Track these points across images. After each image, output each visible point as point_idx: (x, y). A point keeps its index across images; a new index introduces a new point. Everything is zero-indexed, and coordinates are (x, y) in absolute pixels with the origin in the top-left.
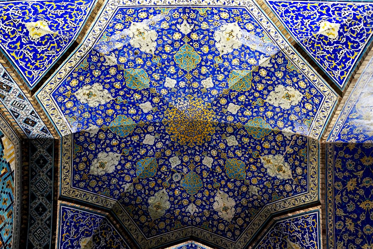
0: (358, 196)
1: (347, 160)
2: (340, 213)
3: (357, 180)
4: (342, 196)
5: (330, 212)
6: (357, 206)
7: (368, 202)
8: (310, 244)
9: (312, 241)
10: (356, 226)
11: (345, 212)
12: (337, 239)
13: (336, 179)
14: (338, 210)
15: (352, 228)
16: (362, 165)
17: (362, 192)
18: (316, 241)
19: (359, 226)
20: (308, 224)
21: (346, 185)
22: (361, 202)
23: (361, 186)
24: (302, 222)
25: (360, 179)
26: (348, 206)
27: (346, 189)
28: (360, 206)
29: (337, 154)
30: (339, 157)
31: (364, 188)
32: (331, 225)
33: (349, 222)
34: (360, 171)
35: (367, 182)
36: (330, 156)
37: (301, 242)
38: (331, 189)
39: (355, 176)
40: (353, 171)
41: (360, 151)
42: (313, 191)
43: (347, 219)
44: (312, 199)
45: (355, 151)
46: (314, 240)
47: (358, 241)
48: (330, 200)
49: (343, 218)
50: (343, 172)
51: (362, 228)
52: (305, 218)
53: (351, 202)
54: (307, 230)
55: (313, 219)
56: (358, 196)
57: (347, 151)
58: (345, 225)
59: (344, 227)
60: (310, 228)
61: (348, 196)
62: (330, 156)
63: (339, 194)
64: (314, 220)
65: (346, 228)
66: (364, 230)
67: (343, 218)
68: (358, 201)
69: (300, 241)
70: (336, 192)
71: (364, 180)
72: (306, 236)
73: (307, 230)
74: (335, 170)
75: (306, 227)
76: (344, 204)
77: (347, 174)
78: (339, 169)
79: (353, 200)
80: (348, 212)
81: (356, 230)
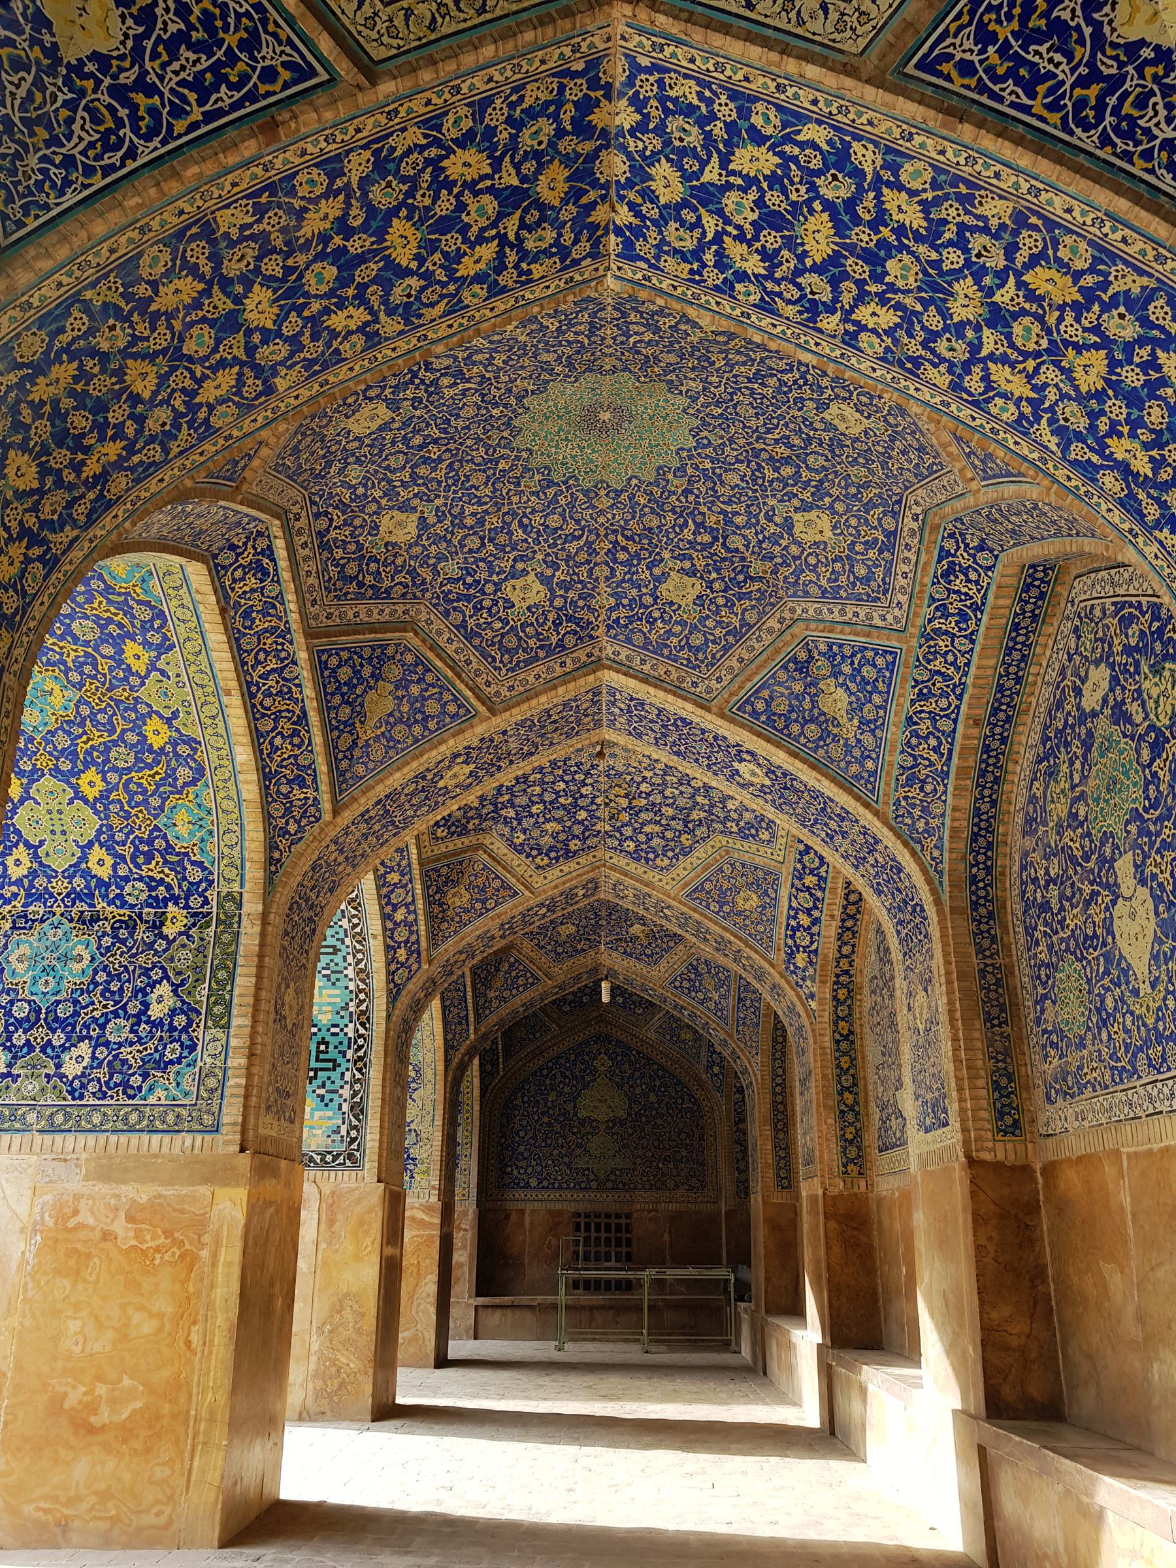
0: (427, 202)
1: (556, 117)
2: (358, 166)
3: (483, 178)
4: (422, 148)
5: (351, 132)
6: (393, 212)
7: (411, 238)
8: (172, 90)
9: (192, 97)
10: (325, 238)
11: (364, 182)
12: (258, 194)
13: (481, 106)
14: (367, 154)
15: (313, 225)
16: (539, 171)
17: (445, 205)
18: (209, 117)
19: (326, 246)
20: (251, 44)
21: (463, 146)
22: (409, 218)
23: (467, 197)
24: (238, 16)
25: (489, 183)
26: (389, 185)
27: (450, 152)
28: (395, 221)
29: (574, 75)
30: (562, 87)
31: (461, 207)
32: (304, 153)
33: (332, 208)
34: (518, 173)
35: (481, 211)
36: (567, 51)
37: (149, 44)
38: (440, 101)
39: (496, 165)
40: (515, 149)
41: (588, 147)
42: (399, 21)
43: (341, 197)
44: (366, 32)
45: (582, 128)
46: (201, 102)
47: (273, 267)
48: (396, 111)
49: (339, 183)
50: (510, 121)
51: (320, 257)
52: (264, 21)
53: (405, 188)
54: (220, 54)
55: (284, 65)
56: (427, 202)
57: (586, 106)
58: (316, 201)
59: (310, 200)
60: (241, 66)
61: (423, 170)
62: (567, 51)
63: (426, 136)
64: (285, 75)
65: (305, 210)
66: (317, 267)
67: (339, 183)
68: (412, 209)
69: (146, 35)
70: (433, 123)
71: (486, 199)
72: (193, 57)
73: (220, 54)
74: (515, 90)
75: (231, 39)
76: (391, 166)
77: (505, 135)
78: (521, 99)
79: (410, 194)
80: (365, 194)
81: (308, 242)
